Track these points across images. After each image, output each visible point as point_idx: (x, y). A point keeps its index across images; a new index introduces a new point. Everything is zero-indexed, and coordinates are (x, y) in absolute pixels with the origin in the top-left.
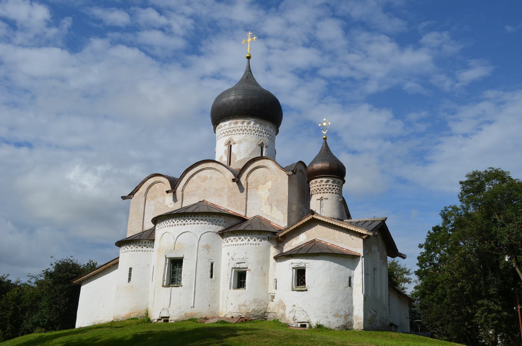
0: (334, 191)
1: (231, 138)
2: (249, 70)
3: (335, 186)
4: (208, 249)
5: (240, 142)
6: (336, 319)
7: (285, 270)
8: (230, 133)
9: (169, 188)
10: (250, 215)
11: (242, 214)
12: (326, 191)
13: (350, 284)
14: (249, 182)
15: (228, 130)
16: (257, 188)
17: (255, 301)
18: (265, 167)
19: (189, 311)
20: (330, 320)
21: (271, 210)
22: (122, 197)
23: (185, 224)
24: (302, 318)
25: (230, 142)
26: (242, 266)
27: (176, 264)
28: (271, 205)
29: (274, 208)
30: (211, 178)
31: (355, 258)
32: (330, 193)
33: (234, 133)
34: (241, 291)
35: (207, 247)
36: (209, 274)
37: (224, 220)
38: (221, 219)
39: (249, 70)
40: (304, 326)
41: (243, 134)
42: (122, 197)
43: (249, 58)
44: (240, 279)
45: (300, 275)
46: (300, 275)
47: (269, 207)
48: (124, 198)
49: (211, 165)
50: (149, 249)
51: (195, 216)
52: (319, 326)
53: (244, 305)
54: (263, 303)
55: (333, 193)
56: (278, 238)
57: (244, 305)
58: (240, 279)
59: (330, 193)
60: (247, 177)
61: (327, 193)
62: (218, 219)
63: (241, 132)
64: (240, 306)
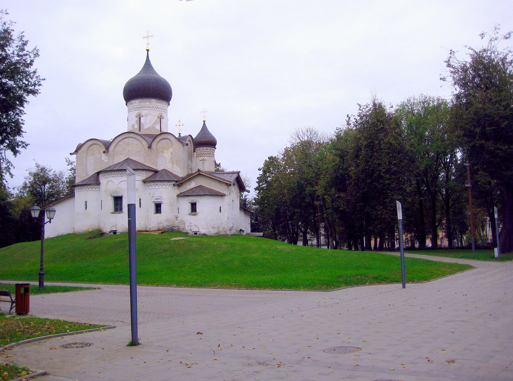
1: (140, 112)
7: (185, 204)
15: (138, 107)
16: (163, 152)
17: (167, 220)
18: (168, 139)
21: (173, 166)
24: (195, 229)
25: (139, 115)
26: (159, 200)
28: (172, 163)
29: (175, 165)
30: (132, 144)
33: (142, 109)
40: (196, 234)
43: (148, 50)
44: (158, 208)
45: (194, 206)
46: (194, 206)
52: (204, 234)
53: (161, 223)
56: (179, 183)
57: (161, 223)
58: (158, 208)
64: (158, 223)
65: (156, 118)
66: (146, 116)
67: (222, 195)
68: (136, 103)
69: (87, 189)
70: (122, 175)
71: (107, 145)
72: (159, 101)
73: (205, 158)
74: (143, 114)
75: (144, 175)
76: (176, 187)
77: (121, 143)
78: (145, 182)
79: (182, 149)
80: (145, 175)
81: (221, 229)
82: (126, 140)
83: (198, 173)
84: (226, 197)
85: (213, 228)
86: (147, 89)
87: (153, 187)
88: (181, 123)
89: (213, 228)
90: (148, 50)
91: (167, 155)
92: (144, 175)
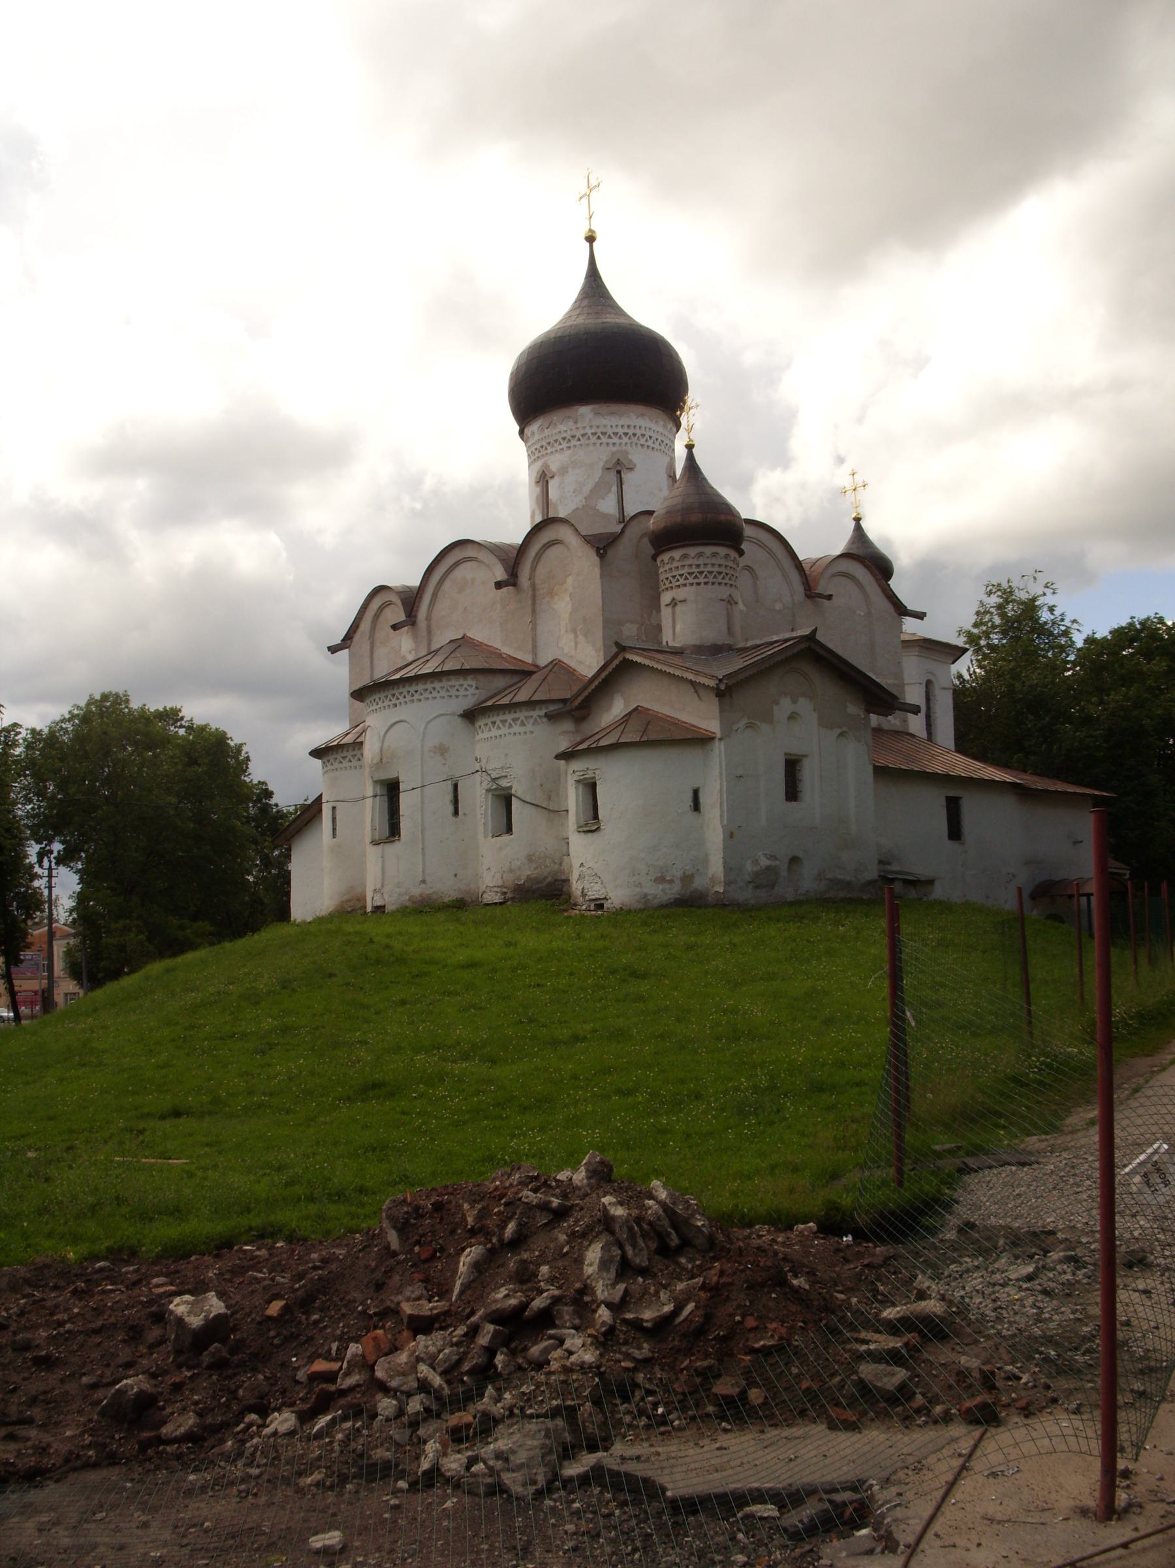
0: (701, 580)
2: (593, 274)
3: (705, 565)
4: (442, 754)
5: (564, 471)
6: (661, 887)
8: (543, 452)
9: (402, 617)
10: (542, 662)
11: (528, 659)
12: (682, 581)
13: (696, 806)
14: (538, 581)
19: (417, 891)
20: (646, 891)
21: (576, 643)
22: (329, 648)
23: (395, 705)
27: (392, 789)
28: (574, 631)
29: (581, 638)
31: (702, 740)
32: (692, 584)
34: (506, 838)
35: (442, 750)
36: (451, 808)
37: (474, 683)
38: (466, 683)
39: (593, 274)
40: (600, 907)
41: (569, 448)
42: (329, 648)
43: (591, 239)
47: (572, 636)
48: (333, 649)
49: (469, 552)
50: (355, 763)
51: (411, 685)
53: (511, 871)
54: (548, 861)
55: (698, 584)
59: (692, 584)
60: (533, 569)
61: (685, 585)
62: (461, 682)
63: (564, 445)
65: (597, 474)
66: (564, 471)
67: (702, 740)
68: (534, 428)
69: (336, 765)
70: (394, 701)
71: (411, 600)
72: (604, 408)
73: (680, 594)
74: (554, 467)
75: (468, 694)
76: (568, 726)
77: (447, 585)
78: (471, 716)
79: (597, 570)
80: (472, 690)
81: (698, 883)
82: (459, 573)
83: (620, 658)
84: (718, 748)
85: (660, 880)
86: (594, 372)
87: (486, 735)
88: (859, 479)
89: (660, 880)
90: (591, 239)
91: (562, 607)
92: (468, 694)
